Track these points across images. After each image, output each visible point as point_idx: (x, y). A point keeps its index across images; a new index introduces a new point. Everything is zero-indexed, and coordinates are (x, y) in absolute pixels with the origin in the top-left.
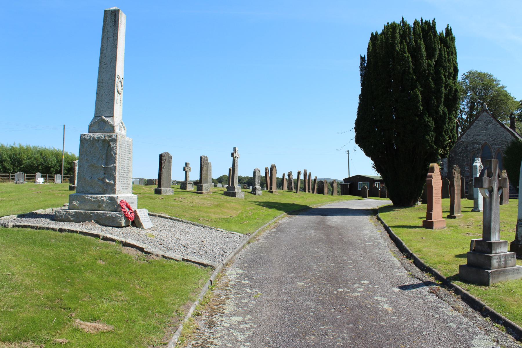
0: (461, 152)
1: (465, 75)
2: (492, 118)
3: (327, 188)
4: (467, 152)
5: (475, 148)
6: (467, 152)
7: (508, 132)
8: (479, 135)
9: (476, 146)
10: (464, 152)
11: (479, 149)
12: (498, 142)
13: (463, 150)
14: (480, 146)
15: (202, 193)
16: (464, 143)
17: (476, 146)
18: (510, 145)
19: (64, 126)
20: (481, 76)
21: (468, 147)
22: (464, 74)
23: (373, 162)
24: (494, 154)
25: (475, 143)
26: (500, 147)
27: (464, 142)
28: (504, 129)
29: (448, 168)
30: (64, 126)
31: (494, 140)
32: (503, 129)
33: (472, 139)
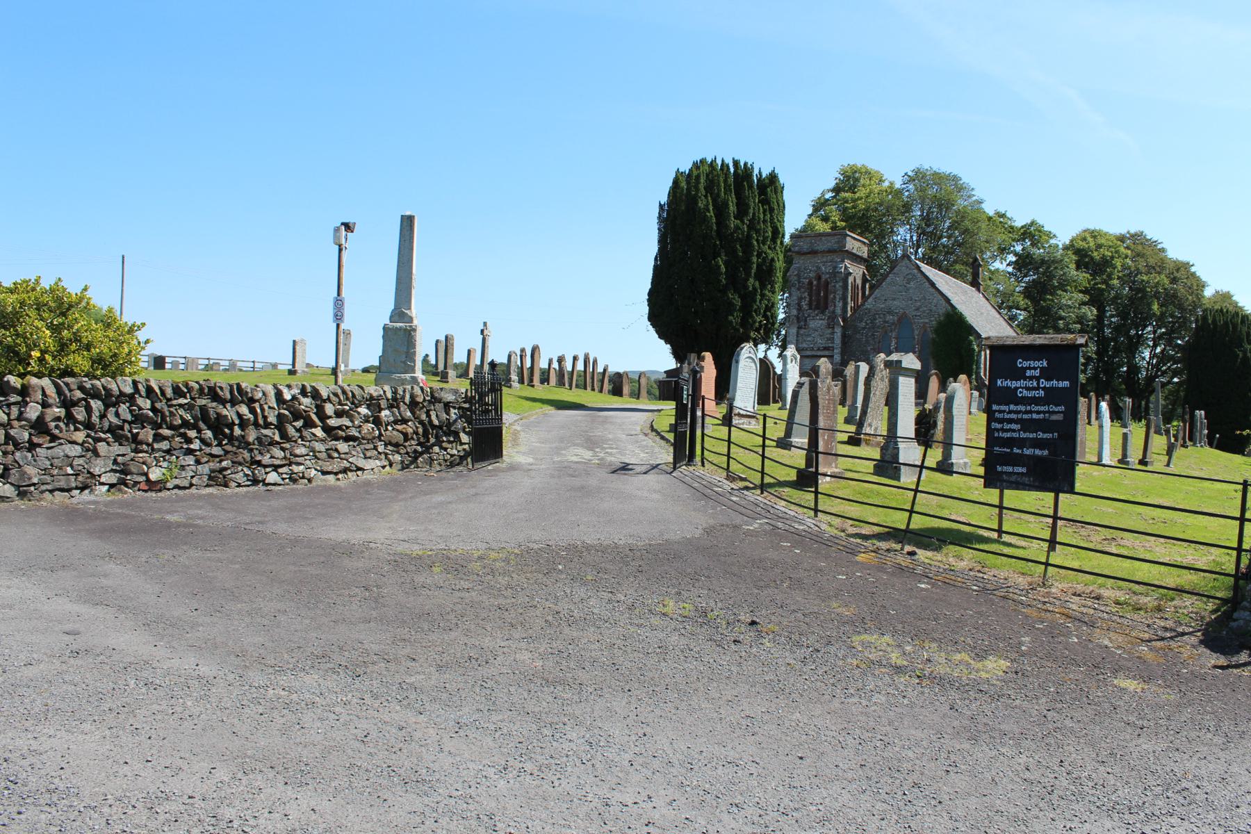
0: (864, 328)
1: (909, 176)
2: (916, 271)
3: (627, 387)
4: (873, 328)
5: (887, 322)
6: (873, 328)
7: (940, 297)
8: (894, 299)
9: (889, 318)
10: (869, 328)
11: (893, 324)
12: (924, 312)
13: (867, 324)
14: (896, 318)
15: (448, 382)
16: (869, 312)
17: (889, 318)
18: (942, 318)
19: (123, 257)
20: (939, 178)
21: (875, 319)
22: (906, 174)
23: (669, 346)
24: (916, 332)
25: (888, 313)
26: (927, 321)
27: (869, 310)
28: (934, 290)
29: (841, 354)
30: (123, 257)
31: (918, 309)
32: (932, 290)
33: (883, 306)
